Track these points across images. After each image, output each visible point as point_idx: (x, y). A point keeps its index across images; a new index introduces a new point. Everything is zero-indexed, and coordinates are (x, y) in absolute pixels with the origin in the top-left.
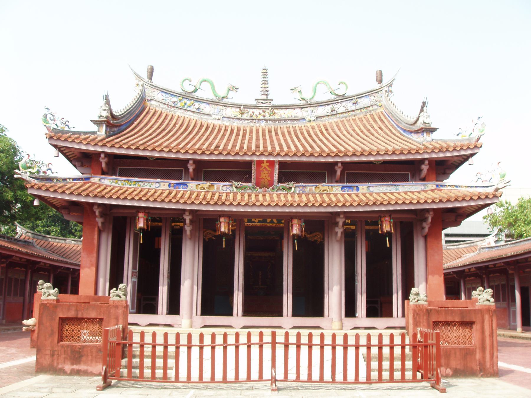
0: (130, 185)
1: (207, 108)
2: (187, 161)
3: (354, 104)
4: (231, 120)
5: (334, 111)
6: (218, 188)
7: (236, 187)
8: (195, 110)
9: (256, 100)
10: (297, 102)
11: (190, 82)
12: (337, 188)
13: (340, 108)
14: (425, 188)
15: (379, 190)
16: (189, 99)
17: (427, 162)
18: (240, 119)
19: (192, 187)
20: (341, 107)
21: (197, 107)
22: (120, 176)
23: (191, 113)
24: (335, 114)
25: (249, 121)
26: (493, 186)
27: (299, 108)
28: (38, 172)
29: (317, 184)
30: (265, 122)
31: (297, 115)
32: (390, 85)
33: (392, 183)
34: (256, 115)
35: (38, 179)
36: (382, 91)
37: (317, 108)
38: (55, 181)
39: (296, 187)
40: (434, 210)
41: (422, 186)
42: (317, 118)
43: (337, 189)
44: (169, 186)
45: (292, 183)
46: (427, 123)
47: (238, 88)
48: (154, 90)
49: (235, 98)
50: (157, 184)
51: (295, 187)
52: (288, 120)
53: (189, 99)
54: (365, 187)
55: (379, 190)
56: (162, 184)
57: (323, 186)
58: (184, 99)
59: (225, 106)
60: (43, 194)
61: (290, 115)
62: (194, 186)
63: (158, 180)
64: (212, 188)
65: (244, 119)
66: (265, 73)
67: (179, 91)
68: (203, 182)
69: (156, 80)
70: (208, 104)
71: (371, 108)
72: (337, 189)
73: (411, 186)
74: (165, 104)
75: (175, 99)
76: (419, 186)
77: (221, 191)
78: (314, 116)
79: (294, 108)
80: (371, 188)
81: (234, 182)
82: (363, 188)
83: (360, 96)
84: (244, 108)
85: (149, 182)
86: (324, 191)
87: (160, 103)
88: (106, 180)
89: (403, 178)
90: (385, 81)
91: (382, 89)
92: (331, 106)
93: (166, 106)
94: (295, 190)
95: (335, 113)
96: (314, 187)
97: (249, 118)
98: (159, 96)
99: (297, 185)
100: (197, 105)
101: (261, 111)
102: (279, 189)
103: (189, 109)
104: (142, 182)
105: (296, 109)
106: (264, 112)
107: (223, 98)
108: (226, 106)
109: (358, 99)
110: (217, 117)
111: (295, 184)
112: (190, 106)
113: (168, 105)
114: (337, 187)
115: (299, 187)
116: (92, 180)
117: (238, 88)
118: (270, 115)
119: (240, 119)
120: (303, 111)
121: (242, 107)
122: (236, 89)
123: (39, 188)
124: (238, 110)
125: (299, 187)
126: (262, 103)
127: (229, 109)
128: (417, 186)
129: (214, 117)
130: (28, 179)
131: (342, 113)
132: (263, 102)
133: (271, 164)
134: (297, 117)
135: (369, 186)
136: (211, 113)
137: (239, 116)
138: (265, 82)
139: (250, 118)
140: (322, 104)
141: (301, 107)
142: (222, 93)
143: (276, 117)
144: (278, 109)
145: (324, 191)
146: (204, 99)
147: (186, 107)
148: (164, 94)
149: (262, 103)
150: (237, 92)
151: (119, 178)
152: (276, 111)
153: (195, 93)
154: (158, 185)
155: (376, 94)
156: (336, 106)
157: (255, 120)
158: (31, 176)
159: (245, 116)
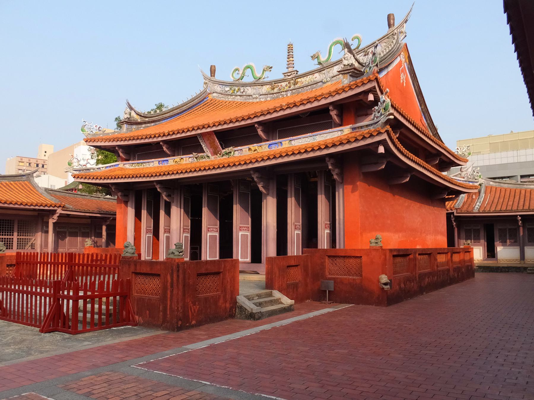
0: (139, 166)
1: (249, 90)
3: (367, 56)
4: (266, 96)
6: (186, 160)
7: (196, 158)
8: (241, 94)
9: (283, 74)
11: (239, 71)
15: (300, 143)
16: (237, 86)
17: (331, 108)
21: (242, 91)
22: (138, 160)
23: (239, 97)
25: (279, 94)
29: (249, 146)
30: (291, 92)
31: (315, 79)
32: (401, 25)
33: (310, 134)
37: (332, 68)
39: (235, 151)
41: (339, 132)
42: (333, 77)
43: (265, 148)
45: (231, 148)
46: (346, 64)
47: (271, 68)
48: (215, 84)
50: (153, 163)
51: (235, 151)
53: (237, 86)
55: (300, 143)
57: (253, 146)
58: (234, 87)
59: (262, 86)
60: (82, 180)
61: (309, 81)
62: (172, 161)
63: (153, 160)
65: (275, 93)
66: (290, 48)
68: (177, 157)
69: (218, 77)
72: (265, 148)
73: (329, 134)
74: (222, 94)
75: (227, 89)
76: (337, 132)
77: (188, 162)
78: (330, 76)
79: (314, 73)
80: (293, 142)
81: (194, 153)
84: (275, 84)
87: (219, 94)
88: (127, 165)
91: (392, 33)
93: (223, 95)
96: (247, 149)
98: (218, 88)
101: (287, 83)
102: (223, 156)
104: (145, 163)
105: (315, 74)
106: (289, 83)
108: (263, 85)
111: (233, 149)
113: (224, 94)
114: (265, 146)
115: (238, 150)
116: (120, 166)
117: (271, 68)
119: (272, 94)
120: (321, 75)
121: (273, 83)
126: (287, 75)
127: (264, 87)
129: (254, 96)
132: (289, 74)
134: (316, 81)
136: (252, 94)
137: (272, 92)
138: (290, 56)
139: (280, 91)
140: (337, 63)
141: (319, 71)
142: (258, 75)
144: (300, 78)
146: (247, 83)
147: (235, 92)
148: (221, 86)
149: (289, 76)
150: (271, 71)
152: (299, 80)
153: (241, 80)
155: (387, 39)
157: (284, 92)
159: (276, 90)
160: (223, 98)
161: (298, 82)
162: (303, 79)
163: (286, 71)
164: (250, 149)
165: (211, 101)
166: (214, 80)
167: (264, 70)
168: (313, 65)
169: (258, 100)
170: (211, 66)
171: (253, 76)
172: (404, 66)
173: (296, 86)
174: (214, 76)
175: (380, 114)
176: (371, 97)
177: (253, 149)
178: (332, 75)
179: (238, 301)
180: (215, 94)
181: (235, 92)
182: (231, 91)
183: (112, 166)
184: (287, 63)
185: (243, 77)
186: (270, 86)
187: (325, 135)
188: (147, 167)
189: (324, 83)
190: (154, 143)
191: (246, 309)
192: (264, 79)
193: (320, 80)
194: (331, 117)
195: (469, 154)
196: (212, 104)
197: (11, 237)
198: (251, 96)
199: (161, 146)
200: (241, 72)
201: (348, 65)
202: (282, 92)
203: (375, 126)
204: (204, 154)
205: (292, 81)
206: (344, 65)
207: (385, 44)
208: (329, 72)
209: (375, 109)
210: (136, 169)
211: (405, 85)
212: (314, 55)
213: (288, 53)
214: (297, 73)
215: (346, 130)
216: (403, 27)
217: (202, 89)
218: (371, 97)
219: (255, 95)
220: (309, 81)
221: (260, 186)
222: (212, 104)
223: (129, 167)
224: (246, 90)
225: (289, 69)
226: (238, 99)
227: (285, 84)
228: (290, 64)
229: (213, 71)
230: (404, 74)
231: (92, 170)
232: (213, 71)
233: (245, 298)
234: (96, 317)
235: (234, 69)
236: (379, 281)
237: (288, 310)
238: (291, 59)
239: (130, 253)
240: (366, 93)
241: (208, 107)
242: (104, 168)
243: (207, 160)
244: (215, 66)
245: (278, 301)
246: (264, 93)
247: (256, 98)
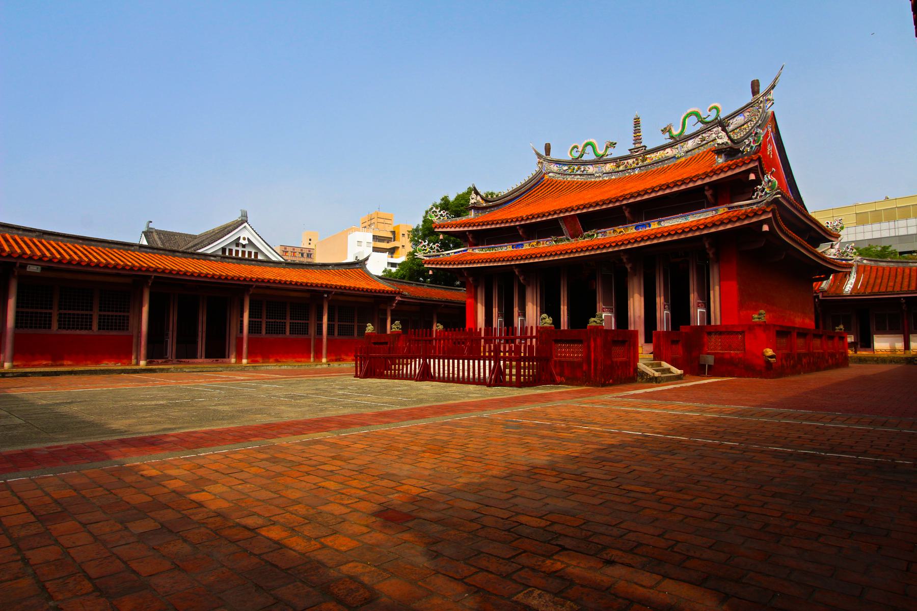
1: (591, 169)
2: (515, 226)
5: (704, 140)
7: (555, 241)
9: (630, 150)
11: (578, 149)
14: (717, 213)
16: (576, 165)
17: (706, 188)
18: (618, 172)
19: (526, 246)
20: (712, 134)
21: (582, 170)
23: (579, 176)
24: (705, 144)
26: (764, 200)
27: (669, 147)
28: (429, 252)
34: (631, 164)
35: (429, 256)
36: (758, 102)
38: (441, 256)
41: (713, 212)
44: (513, 248)
46: (721, 143)
47: (616, 143)
49: (615, 153)
51: (597, 233)
52: (660, 162)
53: (576, 165)
54: (656, 223)
57: (619, 228)
59: (605, 163)
61: (660, 157)
62: (528, 244)
64: (539, 244)
66: (637, 123)
67: (569, 157)
69: (554, 155)
70: (591, 165)
72: (632, 229)
73: (701, 214)
74: (559, 174)
75: (565, 168)
77: (545, 245)
80: (663, 223)
82: (654, 226)
85: (500, 247)
86: (620, 232)
90: (762, 89)
91: (757, 101)
92: (700, 137)
94: (597, 236)
95: (704, 142)
96: (612, 231)
97: (624, 169)
98: (555, 168)
99: (599, 231)
101: (634, 160)
106: (637, 160)
107: (603, 156)
108: (606, 162)
109: (729, 122)
110: (598, 175)
112: (577, 171)
115: (601, 233)
116: (468, 251)
117: (616, 143)
118: (643, 161)
120: (673, 150)
122: (613, 145)
123: (429, 263)
125: (601, 233)
127: (608, 165)
128: (708, 213)
130: (422, 257)
134: (668, 157)
135: (659, 223)
136: (594, 172)
137: (618, 169)
138: (637, 131)
141: (670, 146)
142: (601, 152)
143: (648, 161)
145: (620, 232)
147: (575, 171)
152: (648, 156)
154: (506, 247)
155: (751, 108)
157: (630, 169)
158: (425, 255)
159: (621, 168)
160: (560, 178)
161: (647, 158)
162: (653, 156)
163: (633, 147)
165: (547, 181)
166: (550, 159)
167: (607, 147)
168: (664, 140)
169: (601, 179)
170: (546, 144)
171: (595, 153)
172: (771, 137)
174: (549, 155)
175: (764, 193)
176: (752, 177)
178: (685, 149)
179: (639, 367)
180: (550, 174)
181: (575, 171)
182: (570, 171)
183: (461, 251)
184: (634, 138)
185: (583, 155)
186: (615, 164)
187: (699, 215)
188: (500, 252)
189: (678, 158)
191: (647, 374)
192: (607, 156)
193: (673, 155)
194: (706, 196)
195: (842, 228)
196: (550, 185)
197: (353, 324)
198: (593, 174)
199: (517, 230)
200: (580, 149)
201: (723, 143)
202: (628, 170)
203: (759, 205)
204: (564, 236)
206: (718, 144)
207: (748, 114)
208: (682, 147)
209: (758, 188)
210: (488, 253)
211: (771, 157)
212: (665, 128)
213: (635, 127)
214: (645, 149)
215: (722, 210)
216: (770, 93)
217: (537, 169)
218: (752, 177)
219: (597, 173)
220: (660, 157)
221: (628, 267)
222: (550, 185)
223: (478, 252)
224: (587, 169)
225: (636, 145)
226: (578, 178)
227: (632, 161)
228: (637, 139)
229: (548, 148)
230: (771, 145)
231: (441, 256)
232: (548, 148)
233: (644, 366)
234: (514, 378)
235: (572, 146)
236: (763, 354)
237: (679, 378)
238: (638, 134)
239: (548, 324)
240: (748, 172)
241: (546, 188)
242: (453, 254)
243: (567, 242)
244: (549, 144)
245: (668, 370)
246: (607, 171)
247: (600, 177)
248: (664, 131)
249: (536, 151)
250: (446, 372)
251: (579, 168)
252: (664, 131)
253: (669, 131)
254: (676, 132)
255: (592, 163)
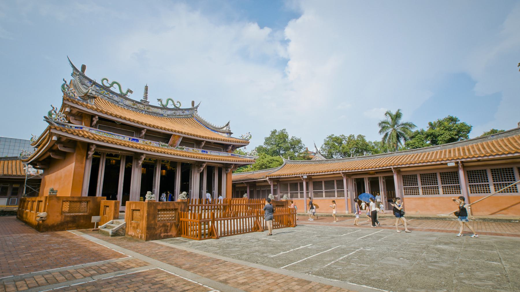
6: (153, 144)
10: (160, 106)
11: (107, 81)
12: (200, 151)
13: (178, 113)
18: (133, 108)
23: (107, 98)
31: (159, 112)
35: (58, 123)
38: (67, 126)
40: (235, 164)
44: (129, 140)
49: (130, 96)
54: (210, 152)
56: (126, 138)
62: (142, 141)
65: (135, 108)
66: (146, 88)
69: (86, 74)
70: (117, 96)
71: (189, 116)
80: (211, 153)
83: (186, 110)
85: (118, 136)
89: (220, 150)
95: (175, 114)
100: (111, 95)
101: (143, 106)
103: (106, 95)
104: (115, 135)
106: (144, 107)
107: (125, 95)
110: (122, 104)
117: (132, 92)
118: (148, 109)
124: (133, 103)
131: (178, 116)
133: (179, 136)
135: (211, 152)
136: (118, 101)
137: (133, 106)
142: (124, 91)
143: (150, 110)
147: (104, 94)
151: (99, 130)
154: (123, 138)
156: (176, 112)
159: (135, 107)
162: (153, 109)
163: (143, 99)
164: (193, 150)
168: (158, 104)
173: (148, 110)
177: (195, 150)
181: (104, 94)
190: (118, 123)
198: (118, 102)
200: (110, 82)
205: (146, 107)
208: (166, 112)
231: (67, 126)
248: (159, 100)
249: (71, 63)
250: (245, 225)
251: (108, 94)
252: (159, 100)
253: (161, 102)
254: (164, 103)
255: (117, 95)
